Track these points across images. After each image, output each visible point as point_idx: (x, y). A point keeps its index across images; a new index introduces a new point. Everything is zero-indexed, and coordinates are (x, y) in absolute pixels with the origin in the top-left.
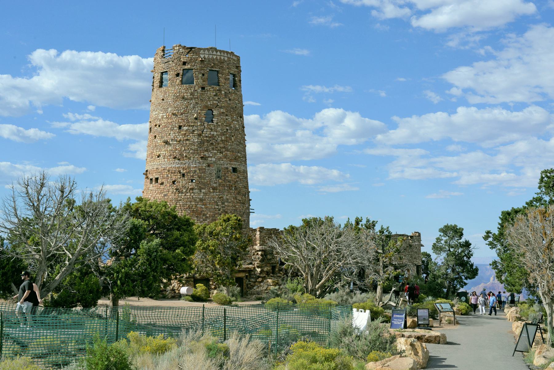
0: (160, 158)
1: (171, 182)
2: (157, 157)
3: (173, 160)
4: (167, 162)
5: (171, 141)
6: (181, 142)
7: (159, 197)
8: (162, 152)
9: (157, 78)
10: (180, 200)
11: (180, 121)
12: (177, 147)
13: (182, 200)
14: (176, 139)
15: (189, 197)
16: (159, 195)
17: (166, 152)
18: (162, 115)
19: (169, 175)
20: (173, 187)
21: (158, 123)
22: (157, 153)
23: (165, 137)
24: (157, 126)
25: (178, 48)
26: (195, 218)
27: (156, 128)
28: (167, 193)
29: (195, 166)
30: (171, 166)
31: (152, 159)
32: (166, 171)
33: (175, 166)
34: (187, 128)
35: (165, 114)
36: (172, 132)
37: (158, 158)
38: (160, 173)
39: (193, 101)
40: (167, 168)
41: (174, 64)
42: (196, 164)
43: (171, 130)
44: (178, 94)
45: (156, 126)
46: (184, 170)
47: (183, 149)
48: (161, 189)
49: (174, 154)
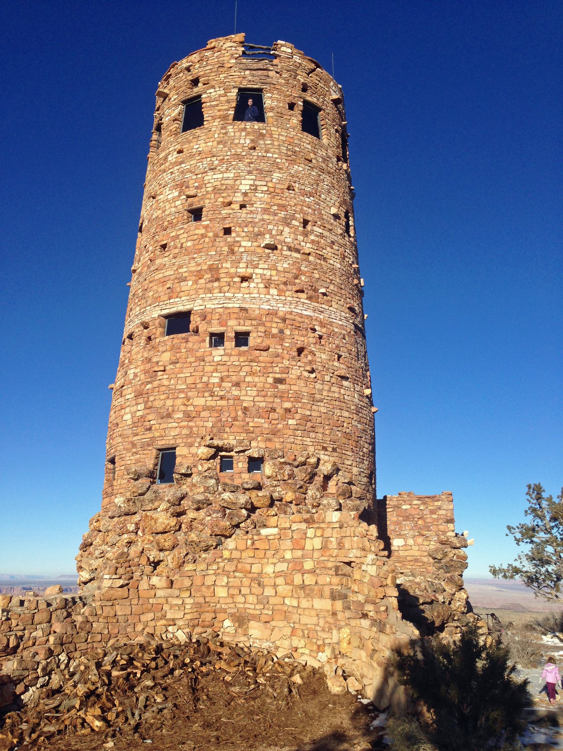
0: (252, 285)
1: (295, 350)
2: (237, 279)
3: (295, 295)
4: (278, 298)
5: (285, 248)
6: (311, 258)
7: (258, 385)
8: (258, 271)
9: (222, 99)
10: (321, 401)
11: (305, 209)
12: (301, 268)
13: (325, 401)
14: (297, 247)
15: (337, 395)
16: (257, 379)
17: (274, 273)
18: (252, 182)
19: (288, 332)
20: (299, 364)
21: (239, 198)
22: (239, 270)
23: (267, 236)
24: (236, 206)
25: (290, 51)
26: (348, 453)
27: (231, 211)
28: (284, 376)
29: (340, 323)
30: (289, 310)
31: (216, 284)
32: (277, 320)
33: (300, 312)
34: (321, 231)
35: (264, 183)
36: (287, 230)
37: (245, 284)
38: (254, 322)
39: (328, 178)
40: (281, 314)
41: (283, 81)
42: (341, 320)
43: (286, 222)
44: (297, 149)
45: (230, 204)
46: (321, 327)
47: (317, 276)
48: (263, 365)
49: (296, 281)
